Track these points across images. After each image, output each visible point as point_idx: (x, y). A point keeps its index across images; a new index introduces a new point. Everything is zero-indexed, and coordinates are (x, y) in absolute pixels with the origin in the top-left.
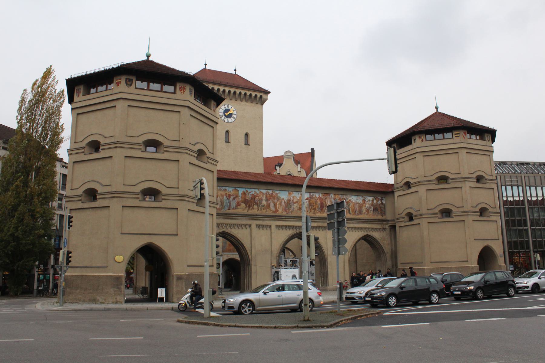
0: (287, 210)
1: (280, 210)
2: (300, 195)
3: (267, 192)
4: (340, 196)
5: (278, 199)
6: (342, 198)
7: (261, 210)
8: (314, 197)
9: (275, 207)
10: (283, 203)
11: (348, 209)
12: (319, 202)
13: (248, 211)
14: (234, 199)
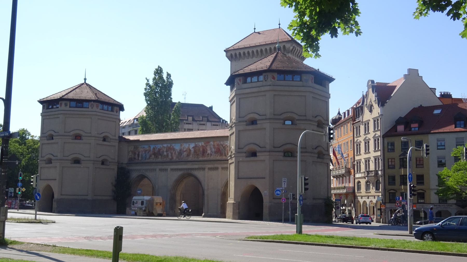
0: (179, 158)
1: (175, 158)
2: (188, 145)
3: (167, 146)
4: (218, 142)
5: (174, 149)
6: (219, 144)
7: (163, 159)
8: (198, 146)
9: (172, 156)
10: (177, 153)
11: (224, 152)
12: (201, 150)
13: (156, 160)
14: (148, 153)
